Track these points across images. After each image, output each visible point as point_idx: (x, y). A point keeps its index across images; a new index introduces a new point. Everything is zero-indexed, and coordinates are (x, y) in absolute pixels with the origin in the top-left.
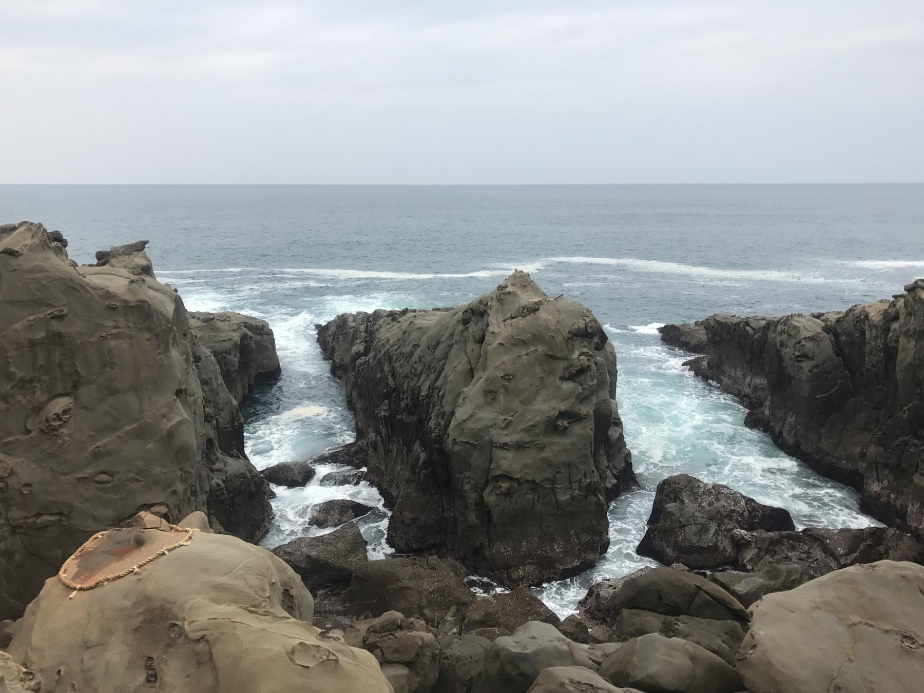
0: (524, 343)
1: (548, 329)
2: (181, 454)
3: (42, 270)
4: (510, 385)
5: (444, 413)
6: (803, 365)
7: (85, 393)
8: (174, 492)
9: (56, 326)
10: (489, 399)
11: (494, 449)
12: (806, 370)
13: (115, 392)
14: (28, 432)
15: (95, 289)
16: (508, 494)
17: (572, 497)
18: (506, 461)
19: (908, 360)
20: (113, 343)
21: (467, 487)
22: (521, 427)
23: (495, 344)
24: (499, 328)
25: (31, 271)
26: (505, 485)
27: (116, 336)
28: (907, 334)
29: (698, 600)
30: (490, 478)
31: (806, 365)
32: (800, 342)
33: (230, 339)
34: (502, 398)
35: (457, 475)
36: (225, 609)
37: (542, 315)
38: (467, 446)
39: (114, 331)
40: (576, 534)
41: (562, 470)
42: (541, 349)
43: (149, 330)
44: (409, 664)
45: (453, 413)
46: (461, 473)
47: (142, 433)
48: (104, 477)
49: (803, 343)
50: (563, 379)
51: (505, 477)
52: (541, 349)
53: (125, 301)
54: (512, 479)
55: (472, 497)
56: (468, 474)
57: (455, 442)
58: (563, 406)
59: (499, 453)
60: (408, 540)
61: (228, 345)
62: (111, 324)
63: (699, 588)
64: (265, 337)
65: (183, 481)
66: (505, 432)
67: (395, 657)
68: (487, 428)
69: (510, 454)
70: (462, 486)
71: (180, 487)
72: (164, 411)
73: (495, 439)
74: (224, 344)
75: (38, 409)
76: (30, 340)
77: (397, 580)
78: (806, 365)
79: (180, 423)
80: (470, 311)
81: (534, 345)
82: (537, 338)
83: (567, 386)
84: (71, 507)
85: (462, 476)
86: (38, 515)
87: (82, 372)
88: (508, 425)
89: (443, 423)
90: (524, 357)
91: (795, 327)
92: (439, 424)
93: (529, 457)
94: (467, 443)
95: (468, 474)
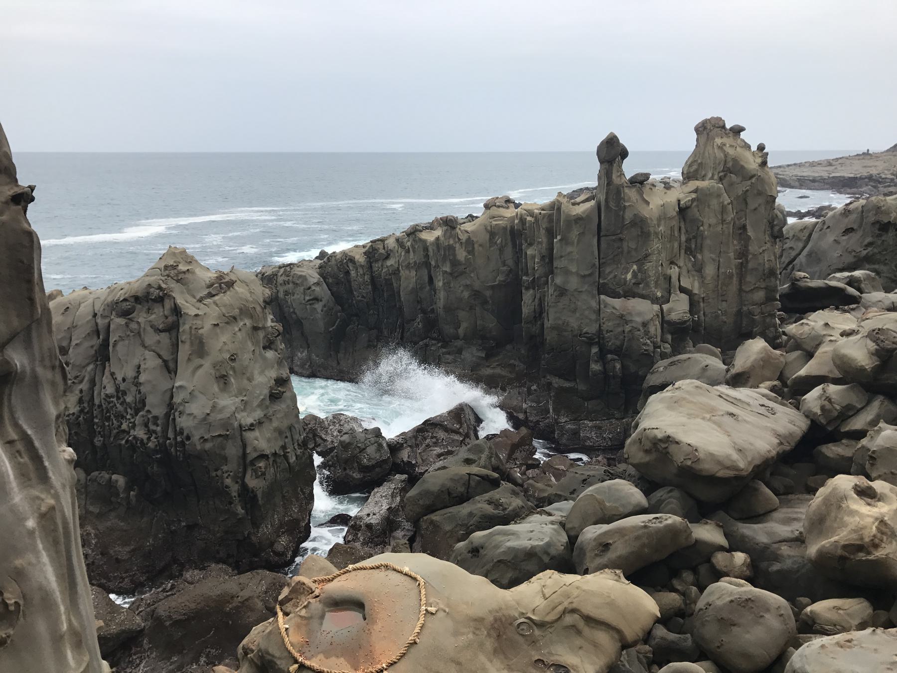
5: (156, 418)
6: (316, 306)
10: (222, 385)
11: (244, 433)
12: (319, 310)
19: (411, 286)
21: (228, 481)
22: (255, 404)
28: (408, 267)
29: (472, 484)
30: (246, 462)
31: (319, 306)
32: (310, 288)
34: (233, 380)
35: (214, 474)
38: (220, 439)
40: (302, 490)
42: (248, 322)
46: (216, 470)
49: (313, 288)
55: (234, 489)
56: (225, 468)
57: (204, 440)
59: (249, 435)
60: (134, 575)
63: (469, 474)
69: (256, 433)
70: (222, 483)
73: (243, 422)
77: (232, 597)
78: (319, 306)
80: (133, 300)
81: (241, 320)
85: (219, 473)
90: (239, 334)
91: (301, 276)
94: (220, 436)
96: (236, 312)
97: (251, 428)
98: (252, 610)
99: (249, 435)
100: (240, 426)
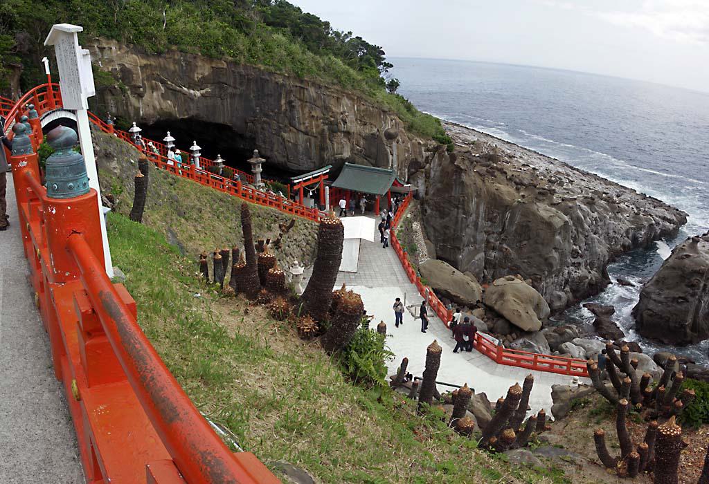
0: (674, 268)
1: (684, 267)
3: (529, 208)
7: (531, 242)
20: (540, 231)
27: (542, 229)
43: (550, 230)
52: (680, 273)
62: (541, 226)
75: (521, 242)
82: (680, 268)
87: (531, 236)
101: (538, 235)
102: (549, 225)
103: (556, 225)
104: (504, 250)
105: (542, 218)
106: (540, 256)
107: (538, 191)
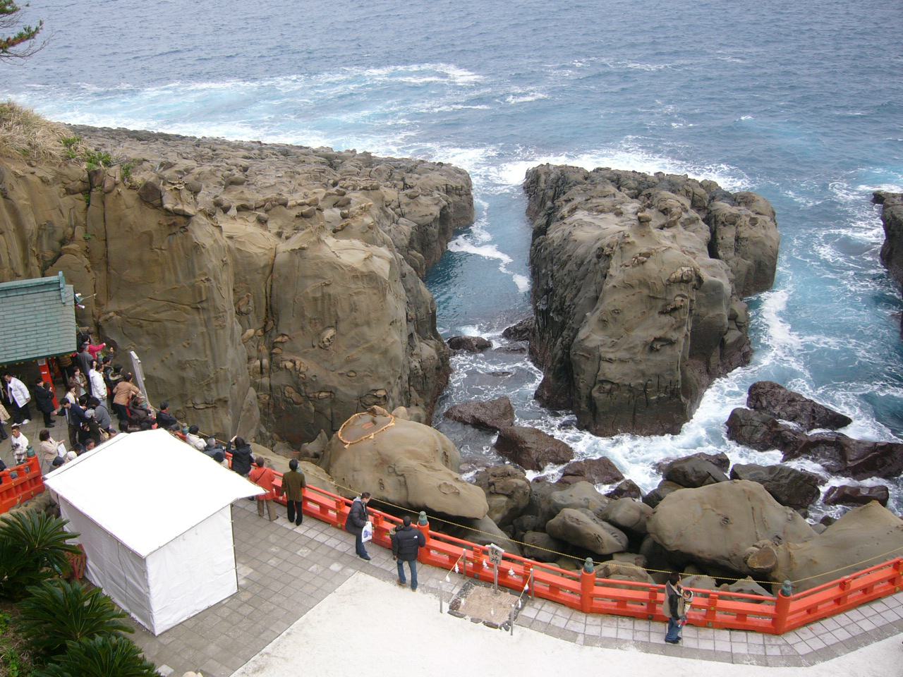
0: (632, 286)
2: (392, 361)
3: (319, 257)
4: (619, 317)
7: (343, 326)
8: (389, 383)
9: (326, 289)
13: (357, 325)
14: (314, 347)
15: (346, 266)
16: (610, 392)
17: (659, 398)
18: (612, 371)
20: (355, 298)
23: (611, 285)
24: (616, 271)
25: (313, 259)
26: (608, 387)
33: (431, 214)
36: (413, 463)
37: (651, 265)
39: (356, 291)
41: (652, 379)
42: (645, 292)
44: (509, 496)
45: (577, 331)
47: (371, 349)
48: (353, 374)
50: (662, 313)
51: (607, 381)
52: (645, 292)
53: (362, 272)
54: (613, 383)
55: (584, 392)
56: (582, 376)
58: (658, 334)
59: (605, 365)
61: (430, 219)
62: (353, 286)
64: (464, 197)
65: (393, 375)
66: (611, 350)
67: (500, 491)
68: (597, 347)
71: (392, 380)
72: (384, 337)
74: (426, 218)
75: (319, 334)
76: (314, 298)
79: (393, 343)
82: (644, 283)
83: (666, 319)
84: (336, 389)
86: (320, 392)
88: (614, 345)
89: (572, 334)
92: (569, 335)
93: (627, 368)
95: (582, 376)
96: (635, 282)
97: (610, 361)
98: (529, 455)
99: (605, 365)
100: (600, 357)
101: (354, 308)
102: (371, 277)
103: (382, 274)
104: (289, 365)
105: (353, 269)
106: (371, 349)
107: (294, 213)
